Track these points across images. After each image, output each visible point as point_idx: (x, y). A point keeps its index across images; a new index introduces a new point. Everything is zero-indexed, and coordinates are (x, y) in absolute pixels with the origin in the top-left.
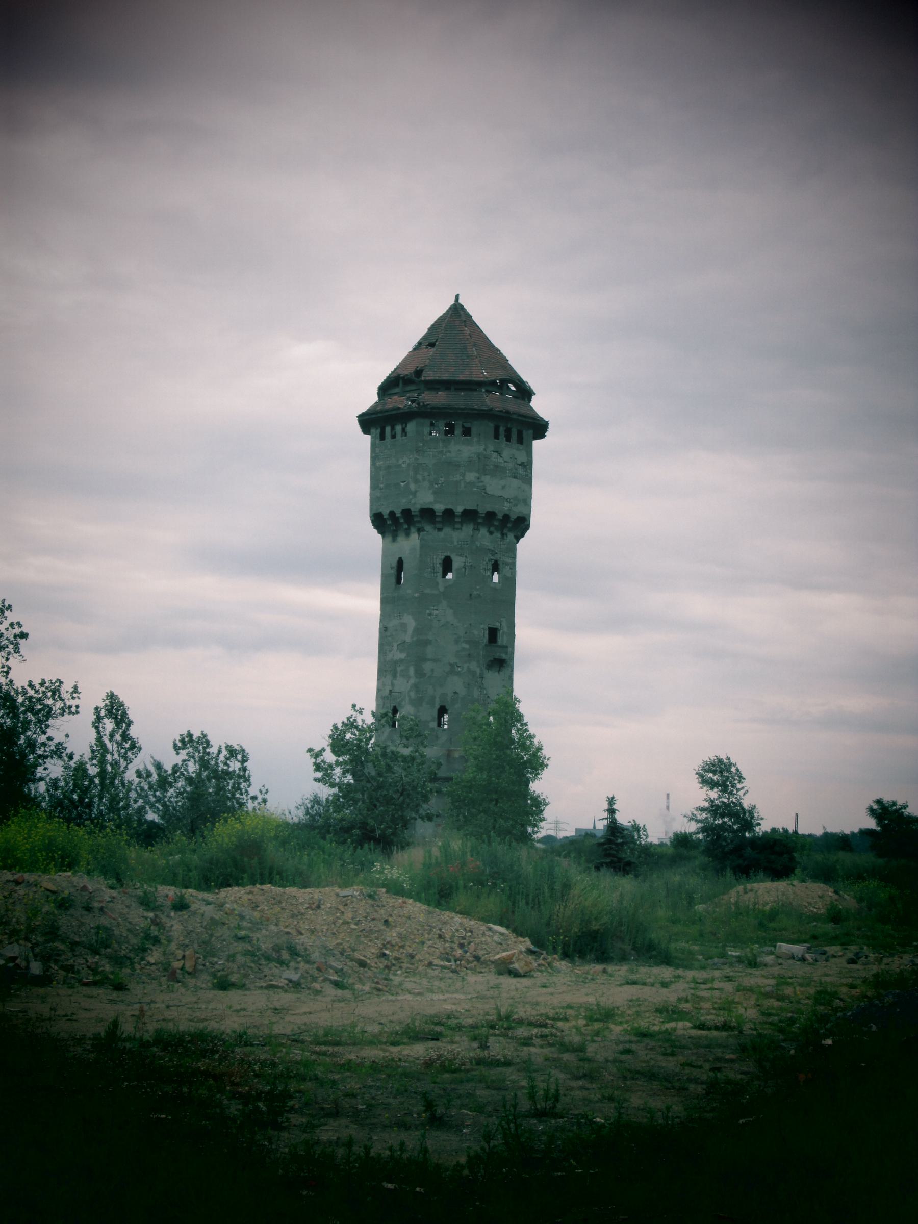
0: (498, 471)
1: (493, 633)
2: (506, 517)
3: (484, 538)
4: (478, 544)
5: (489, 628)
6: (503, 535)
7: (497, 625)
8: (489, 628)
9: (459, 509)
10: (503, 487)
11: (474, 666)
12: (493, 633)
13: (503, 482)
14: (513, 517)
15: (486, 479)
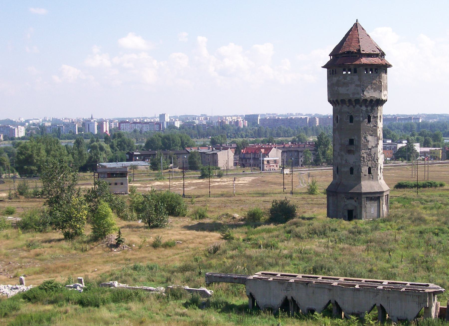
0: (345, 84)
1: (351, 142)
2: (350, 101)
3: (345, 108)
4: (343, 111)
5: (350, 140)
6: (354, 106)
7: (353, 138)
8: (350, 140)
9: (335, 100)
10: (347, 90)
11: (343, 153)
12: (351, 142)
13: (347, 88)
14: (353, 100)
15: (340, 88)
